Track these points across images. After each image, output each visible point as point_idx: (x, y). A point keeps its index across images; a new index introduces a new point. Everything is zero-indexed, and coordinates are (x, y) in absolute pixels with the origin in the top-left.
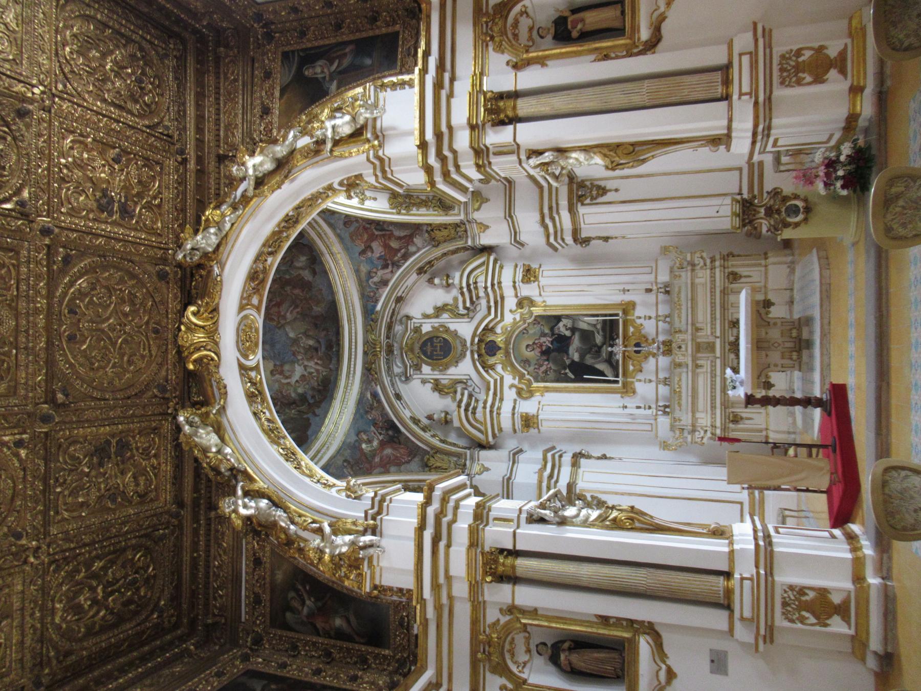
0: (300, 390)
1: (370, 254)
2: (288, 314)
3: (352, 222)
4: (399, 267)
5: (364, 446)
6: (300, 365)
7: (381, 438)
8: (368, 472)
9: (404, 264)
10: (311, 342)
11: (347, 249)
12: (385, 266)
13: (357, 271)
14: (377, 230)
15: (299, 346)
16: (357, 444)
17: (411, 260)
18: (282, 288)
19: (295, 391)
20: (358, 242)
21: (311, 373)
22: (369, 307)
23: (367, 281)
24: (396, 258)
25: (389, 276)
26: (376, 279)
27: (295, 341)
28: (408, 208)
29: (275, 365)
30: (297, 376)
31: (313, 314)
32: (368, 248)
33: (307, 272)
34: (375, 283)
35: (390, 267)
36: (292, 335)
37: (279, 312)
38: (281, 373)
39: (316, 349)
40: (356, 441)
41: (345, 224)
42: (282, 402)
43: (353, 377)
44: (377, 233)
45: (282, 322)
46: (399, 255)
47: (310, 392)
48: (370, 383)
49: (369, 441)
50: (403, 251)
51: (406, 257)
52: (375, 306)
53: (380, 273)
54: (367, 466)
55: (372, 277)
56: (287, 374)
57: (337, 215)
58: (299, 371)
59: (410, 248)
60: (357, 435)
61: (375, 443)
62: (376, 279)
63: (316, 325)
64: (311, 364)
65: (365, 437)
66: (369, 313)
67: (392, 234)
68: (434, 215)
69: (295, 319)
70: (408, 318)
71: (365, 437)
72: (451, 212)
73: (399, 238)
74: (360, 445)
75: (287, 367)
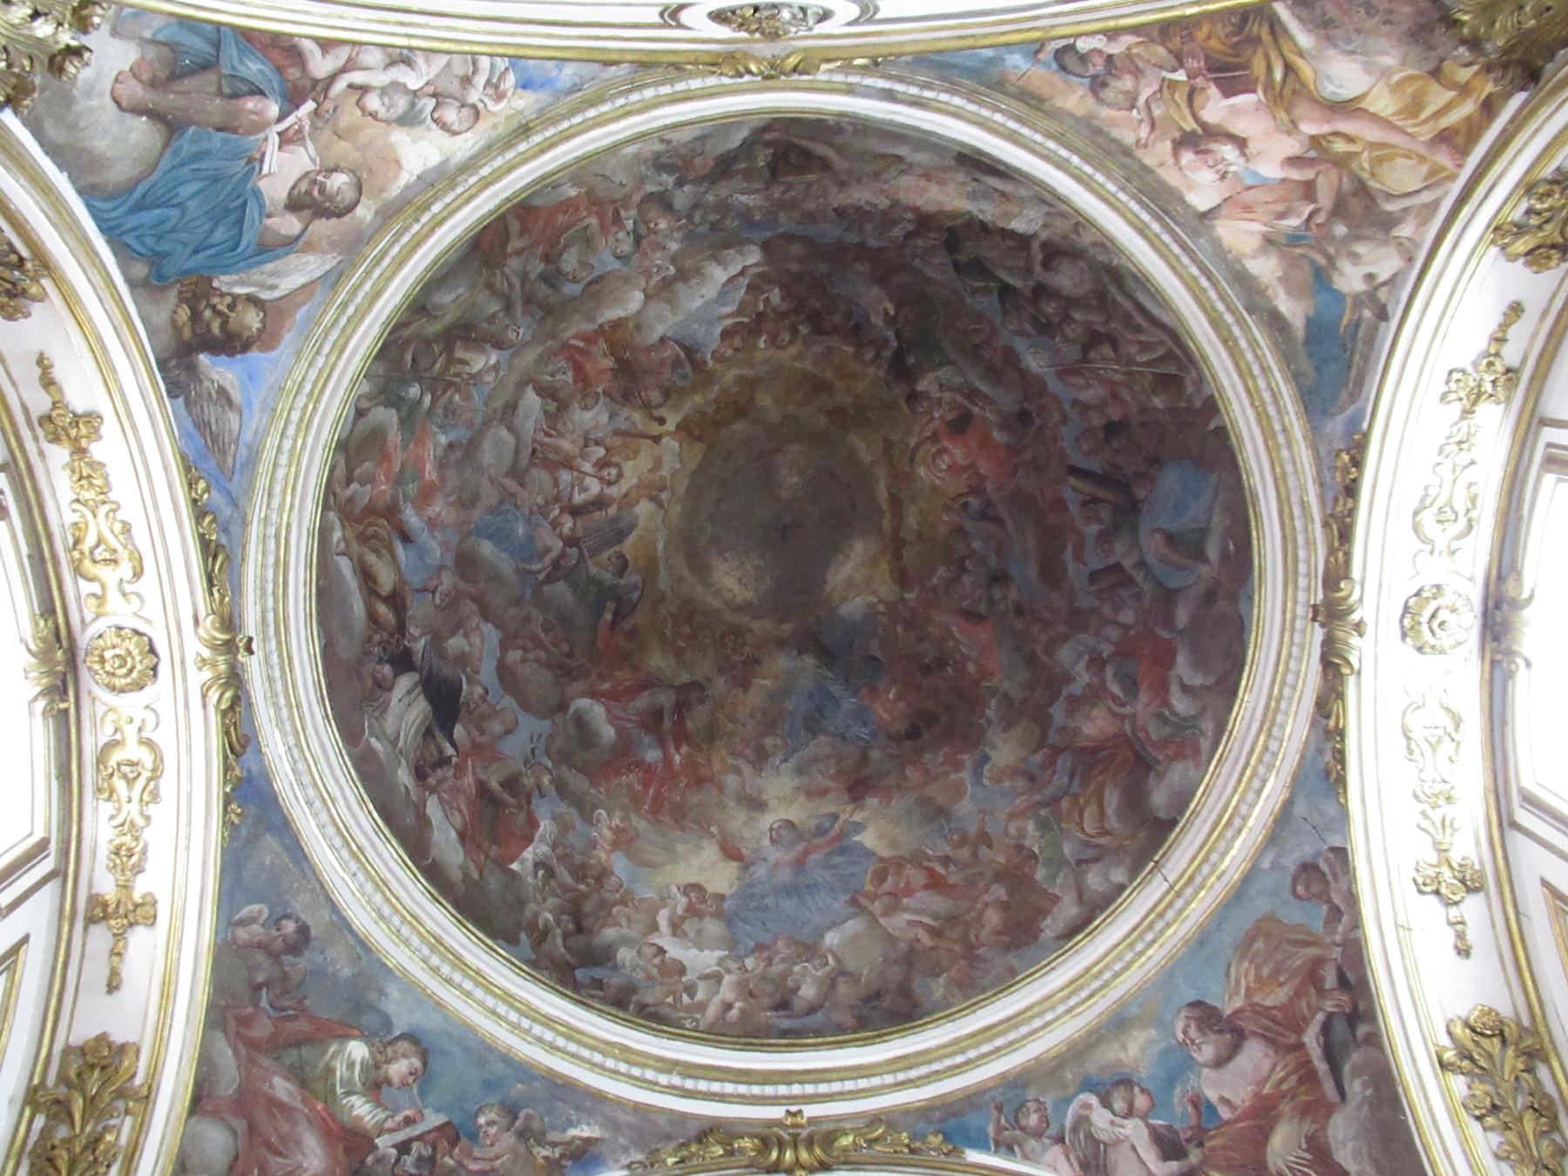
0: (625, 955)
1: (1207, 1052)
2: (907, 916)
3: (1324, 896)
5: (358, 1050)
6: (720, 962)
7: (384, 1143)
8: (226, 1013)
10: (808, 991)
11: (1202, 939)
13: (1118, 1023)
14: (1326, 1029)
15: (791, 961)
16: (368, 1020)
18: (998, 878)
19: (625, 941)
20: (1243, 973)
21: (690, 990)
23: (1088, 1085)
26: (1101, 1119)
27: (809, 950)
28: (1492, 1111)
29: (722, 897)
30: (676, 951)
31: (917, 985)
32: (1229, 1032)
34: (1082, 1121)
36: (832, 939)
37: (909, 891)
38: (692, 911)
39: (783, 1005)
40: (387, 1024)
41: (1308, 869)
42: (586, 896)
43: (672, 1089)
44: (1311, 1038)
45: (877, 907)
47: (615, 980)
48: (641, 1146)
49: (375, 1086)
52: (981, 1144)
53: (1135, 1131)
54: (262, 1029)
55: (1106, 1103)
56: (689, 927)
57: (1332, 810)
58: (700, 959)
60: (411, 1037)
61: (361, 1109)
62: (1101, 1119)
63: (878, 995)
64: (727, 991)
65: (398, 1069)
67: (1330, 1109)
69: (891, 939)
71: (398, 1069)
74: (366, 1036)
75: (713, 927)
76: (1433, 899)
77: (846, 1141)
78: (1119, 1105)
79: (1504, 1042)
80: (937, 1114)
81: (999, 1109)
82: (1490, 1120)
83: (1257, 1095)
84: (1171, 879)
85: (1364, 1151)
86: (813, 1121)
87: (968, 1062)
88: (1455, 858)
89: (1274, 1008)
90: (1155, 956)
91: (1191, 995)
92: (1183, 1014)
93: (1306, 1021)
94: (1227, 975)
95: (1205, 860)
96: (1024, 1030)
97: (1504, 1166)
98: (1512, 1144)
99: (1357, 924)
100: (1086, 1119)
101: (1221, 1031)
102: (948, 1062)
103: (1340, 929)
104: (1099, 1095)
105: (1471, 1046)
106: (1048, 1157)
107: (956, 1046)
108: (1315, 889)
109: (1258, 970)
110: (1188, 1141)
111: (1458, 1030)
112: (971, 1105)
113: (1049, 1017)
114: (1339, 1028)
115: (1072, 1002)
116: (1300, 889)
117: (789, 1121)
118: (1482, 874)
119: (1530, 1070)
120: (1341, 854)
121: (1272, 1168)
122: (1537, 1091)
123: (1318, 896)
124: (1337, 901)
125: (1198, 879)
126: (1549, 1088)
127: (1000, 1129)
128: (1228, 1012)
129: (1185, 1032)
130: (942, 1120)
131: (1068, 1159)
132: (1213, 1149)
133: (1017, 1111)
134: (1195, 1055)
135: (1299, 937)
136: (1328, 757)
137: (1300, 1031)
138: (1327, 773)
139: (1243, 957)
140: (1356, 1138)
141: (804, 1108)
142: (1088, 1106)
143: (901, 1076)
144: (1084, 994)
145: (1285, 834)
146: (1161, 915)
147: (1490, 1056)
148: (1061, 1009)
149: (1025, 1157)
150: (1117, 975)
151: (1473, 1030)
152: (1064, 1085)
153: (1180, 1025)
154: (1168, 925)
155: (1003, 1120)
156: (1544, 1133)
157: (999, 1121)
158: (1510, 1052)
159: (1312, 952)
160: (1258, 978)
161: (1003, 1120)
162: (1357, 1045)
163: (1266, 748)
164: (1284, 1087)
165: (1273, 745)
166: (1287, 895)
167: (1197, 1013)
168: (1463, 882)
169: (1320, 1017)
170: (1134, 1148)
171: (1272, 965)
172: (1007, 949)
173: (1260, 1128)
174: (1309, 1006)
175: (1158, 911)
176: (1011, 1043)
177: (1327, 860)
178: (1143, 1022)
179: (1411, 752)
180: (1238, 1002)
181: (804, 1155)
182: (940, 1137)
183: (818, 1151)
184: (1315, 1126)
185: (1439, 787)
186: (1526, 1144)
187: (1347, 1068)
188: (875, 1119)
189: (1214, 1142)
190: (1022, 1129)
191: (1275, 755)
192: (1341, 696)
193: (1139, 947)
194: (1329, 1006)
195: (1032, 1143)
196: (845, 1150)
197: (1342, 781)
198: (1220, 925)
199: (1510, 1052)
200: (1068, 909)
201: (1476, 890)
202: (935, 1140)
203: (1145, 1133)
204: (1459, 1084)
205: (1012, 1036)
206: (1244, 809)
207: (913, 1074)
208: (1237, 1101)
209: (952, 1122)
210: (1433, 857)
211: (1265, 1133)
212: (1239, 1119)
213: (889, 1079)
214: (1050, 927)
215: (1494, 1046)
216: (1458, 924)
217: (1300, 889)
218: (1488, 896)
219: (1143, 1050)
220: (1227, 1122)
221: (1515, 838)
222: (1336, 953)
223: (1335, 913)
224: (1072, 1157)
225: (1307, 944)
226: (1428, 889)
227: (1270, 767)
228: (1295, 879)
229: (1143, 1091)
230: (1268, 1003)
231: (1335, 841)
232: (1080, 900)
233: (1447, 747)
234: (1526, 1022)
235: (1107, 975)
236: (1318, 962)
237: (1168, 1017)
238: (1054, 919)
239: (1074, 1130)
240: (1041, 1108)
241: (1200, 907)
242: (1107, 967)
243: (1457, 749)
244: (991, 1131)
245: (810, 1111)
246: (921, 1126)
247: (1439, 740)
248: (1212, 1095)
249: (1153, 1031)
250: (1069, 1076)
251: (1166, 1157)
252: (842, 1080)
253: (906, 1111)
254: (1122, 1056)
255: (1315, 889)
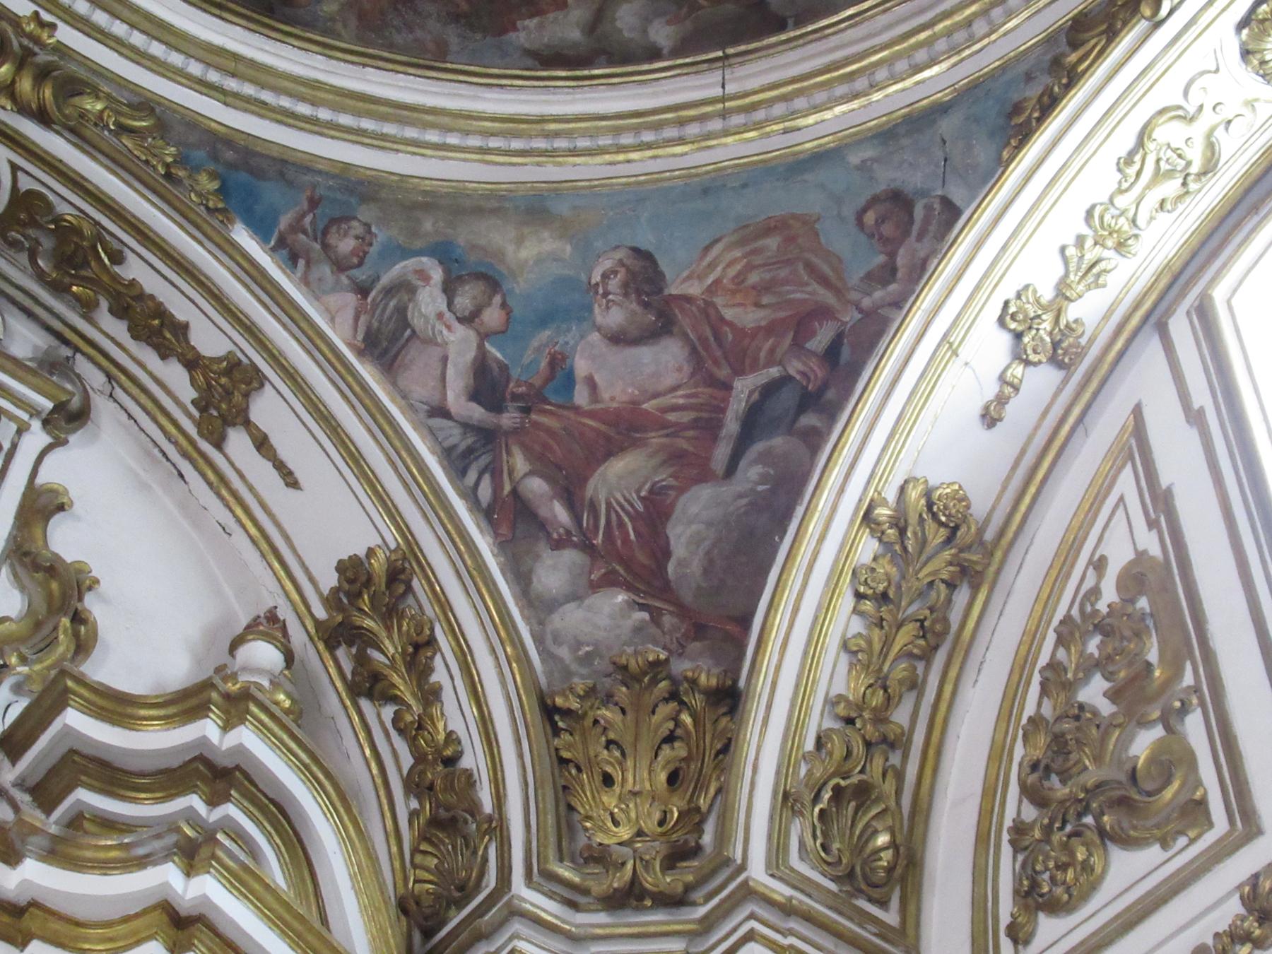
1: (614, 317)
4: (458, 462)
9: (471, 496)
11: (708, 187)
12: (488, 385)
13: (534, 208)
14: (770, 390)
17: (484, 544)
22: (271, 193)
23: (443, 252)
24: (520, 463)
25: (421, 386)
26: (429, 301)
28: (877, 599)
33: (575, 35)
34: (404, 288)
35: (477, 413)
41: (899, 201)
44: (745, 388)
46: (536, 486)
50: (560, 513)
51: (513, 519)
52: (261, 229)
53: (460, 344)
55: (449, 289)
59: (571, 557)
62: (429, 301)
66: (235, 181)
67: (704, 475)
68: (793, 729)
70: (68, 419)
72: (797, 830)
73: (656, 511)
76: (1005, 339)
77: (94, 106)
78: (464, 301)
79: (949, 540)
80: (229, 155)
81: (314, 203)
82: (868, 606)
83: (635, 403)
84: (731, 88)
85: (707, 543)
86: (62, 50)
87: (313, 121)
88: (1072, 312)
89: (730, 324)
90: (641, 164)
91: (646, 240)
92: (619, 255)
93: (754, 367)
94: (707, 249)
95: (785, 98)
96: (411, 133)
97: (844, 659)
98: (869, 642)
99: (899, 303)
100: (412, 290)
101: (646, 305)
102: (285, 102)
103: (878, 294)
104: (447, 272)
105: (913, 519)
106: (334, 300)
107: (311, 90)
108: (888, 229)
109: (750, 268)
110: (515, 397)
111: (914, 494)
112: (282, 174)
113: (453, 140)
114: (787, 398)
115: (494, 143)
116: (870, 217)
117: (31, 28)
118: (1081, 354)
119: (951, 586)
120: (950, 214)
121: (589, 492)
122: (940, 611)
123: (884, 240)
124: (901, 261)
125: (760, 115)
126: (955, 617)
127: (296, 227)
128: (674, 290)
129: (605, 276)
130: (232, 166)
131: (356, 319)
132: (536, 425)
133: (334, 221)
134: (597, 310)
135: (826, 269)
136: (1034, 91)
137: (739, 372)
138: (1017, 109)
139: (742, 242)
140: (709, 524)
141: (60, 24)
142: (424, 276)
143: (213, 76)
144: (516, 144)
145: (905, 142)
146: (682, 123)
147: (923, 543)
148: (474, 141)
149: (305, 282)
150: (574, 152)
151: (930, 505)
152: (414, 233)
153: (607, 264)
154: (681, 141)
155: (308, 219)
156: (910, 655)
157: (303, 216)
158: (947, 554)
159: (828, 297)
160: (739, 279)
161: (308, 219)
162: (790, 431)
163: (969, 23)
164: (672, 417)
165: (980, 27)
166: (849, 211)
167: (637, 264)
168: (1055, 345)
169: (774, 372)
170: (445, 360)
171: (767, 276)
172: (456, 17)
173: (608, 439)
174: (772, 351)
175: (680, 115)
176: (384, 137)
177: (928, 208)
178: (565, 229)
179: (1129, 160)
180: (694, 289)
181: (25, 85)
182: (215, 185)
183: (48, 93)
184: (672, 482)
185: (1123, 223)
186: (884, 653)
187: (758, 447)
188: (146, 104)
189: (544, 420)
190: (326, 247)
191: (972, 40)
192: (1112, 35)
193: (626, 140)
194: (794, 367)
195: (326, 270)
196: (83, 115)
197: (1025, 134)
198: (744, 186)
199: (947, 554)
200: (567, 28)
201: (1060, 365)
202: (208, 184)
203: (471, 354)
204: (867, 548)
205: (390, 129)
206: (881, 74)
207: (232, 84)
208: (606, 395)
209: (243, 177)
210: (1047, 294)
211: (611, 450)
212: (592, 414)
213: (195, 69)
214: (529, 33)
215: (937, 536)
216: (1008, 385)
217: (870, 217)
218: (1065, 381)
219: (539, 260)
220: (577, 409)
221: (1153, 347)
222: (850, 317)
223: (888, 273)
224: (363, 319)
225: (824, 281)
226: (1013, 325)
227: (955, 50)
228: (874, 201)
229: (504, 305)
230: (728, 314)
231: (956, 194)
232: (591, 28)
233: (1171, 187)
234: (989, 536)
235: (561, 143)
236: (823, 313)
237: (598, 244)
238: (541, 26)
239: (389, 291)
240: (366, 238)
241: (735, 148)
242: (568, 134)
243: (1179, 198)
244: (284, 222)
245: (66, 35)
246: (200, 155)
247: (1170, 174)
248: (582, 367)
249: (568, 248)
250: (428, 225)
251: (475, 396)
252: (133, 26)
253: (193, 122)
254: (510, 249)
255: (888, 229)
